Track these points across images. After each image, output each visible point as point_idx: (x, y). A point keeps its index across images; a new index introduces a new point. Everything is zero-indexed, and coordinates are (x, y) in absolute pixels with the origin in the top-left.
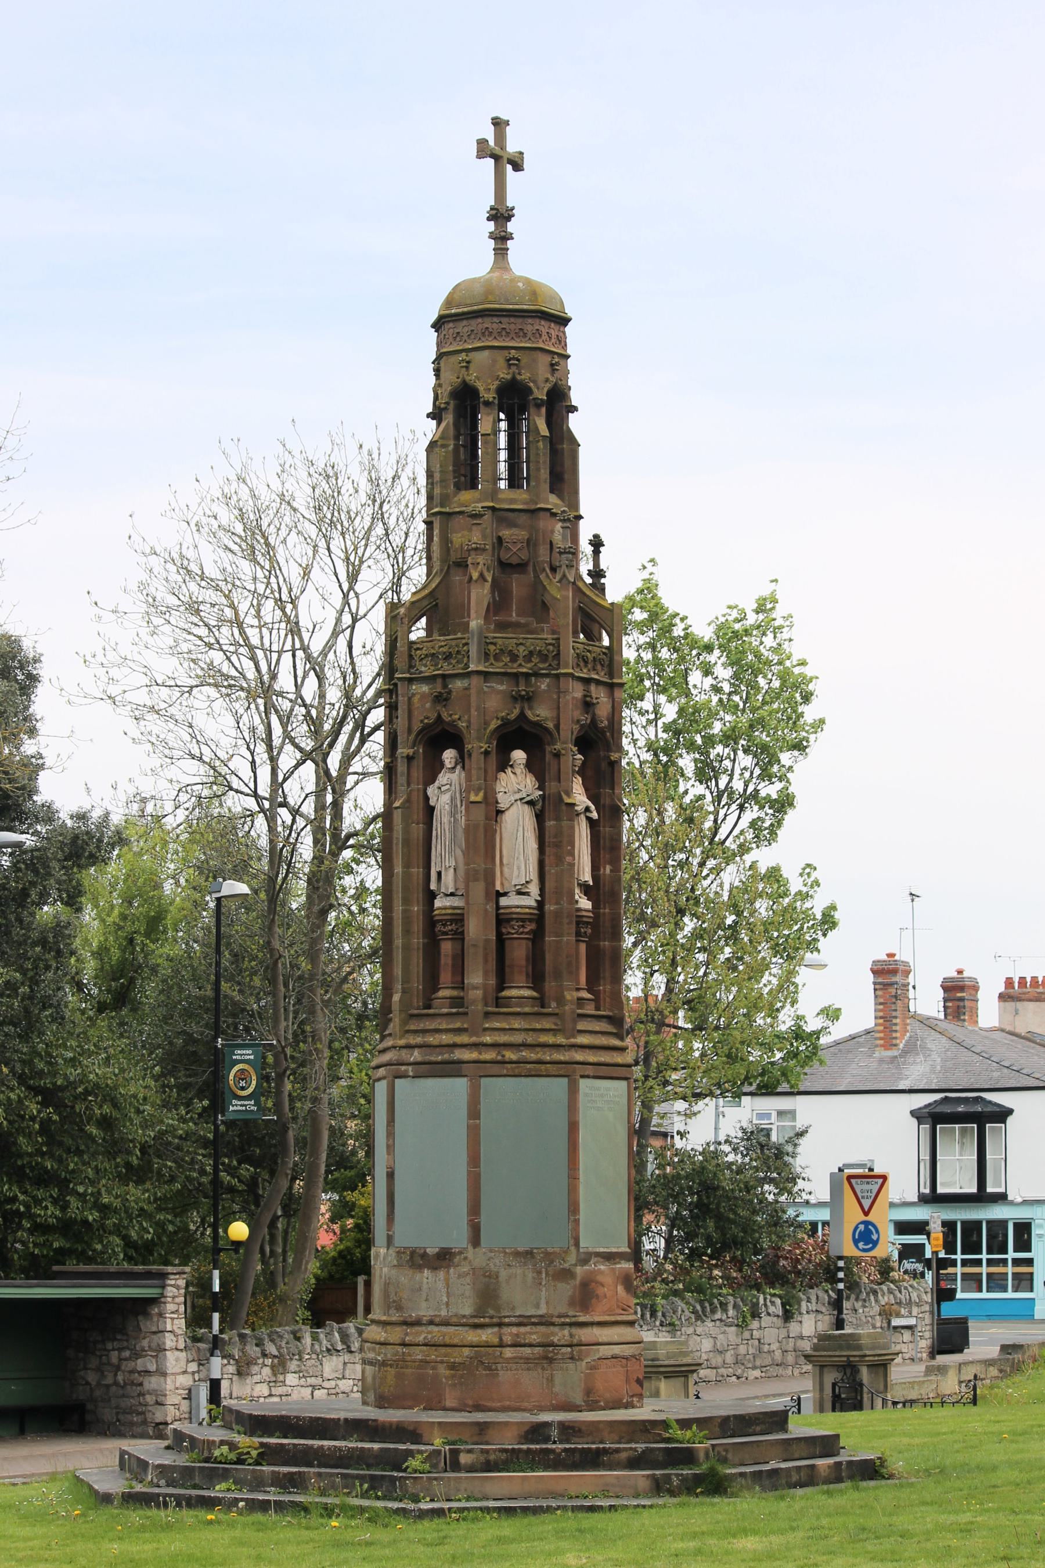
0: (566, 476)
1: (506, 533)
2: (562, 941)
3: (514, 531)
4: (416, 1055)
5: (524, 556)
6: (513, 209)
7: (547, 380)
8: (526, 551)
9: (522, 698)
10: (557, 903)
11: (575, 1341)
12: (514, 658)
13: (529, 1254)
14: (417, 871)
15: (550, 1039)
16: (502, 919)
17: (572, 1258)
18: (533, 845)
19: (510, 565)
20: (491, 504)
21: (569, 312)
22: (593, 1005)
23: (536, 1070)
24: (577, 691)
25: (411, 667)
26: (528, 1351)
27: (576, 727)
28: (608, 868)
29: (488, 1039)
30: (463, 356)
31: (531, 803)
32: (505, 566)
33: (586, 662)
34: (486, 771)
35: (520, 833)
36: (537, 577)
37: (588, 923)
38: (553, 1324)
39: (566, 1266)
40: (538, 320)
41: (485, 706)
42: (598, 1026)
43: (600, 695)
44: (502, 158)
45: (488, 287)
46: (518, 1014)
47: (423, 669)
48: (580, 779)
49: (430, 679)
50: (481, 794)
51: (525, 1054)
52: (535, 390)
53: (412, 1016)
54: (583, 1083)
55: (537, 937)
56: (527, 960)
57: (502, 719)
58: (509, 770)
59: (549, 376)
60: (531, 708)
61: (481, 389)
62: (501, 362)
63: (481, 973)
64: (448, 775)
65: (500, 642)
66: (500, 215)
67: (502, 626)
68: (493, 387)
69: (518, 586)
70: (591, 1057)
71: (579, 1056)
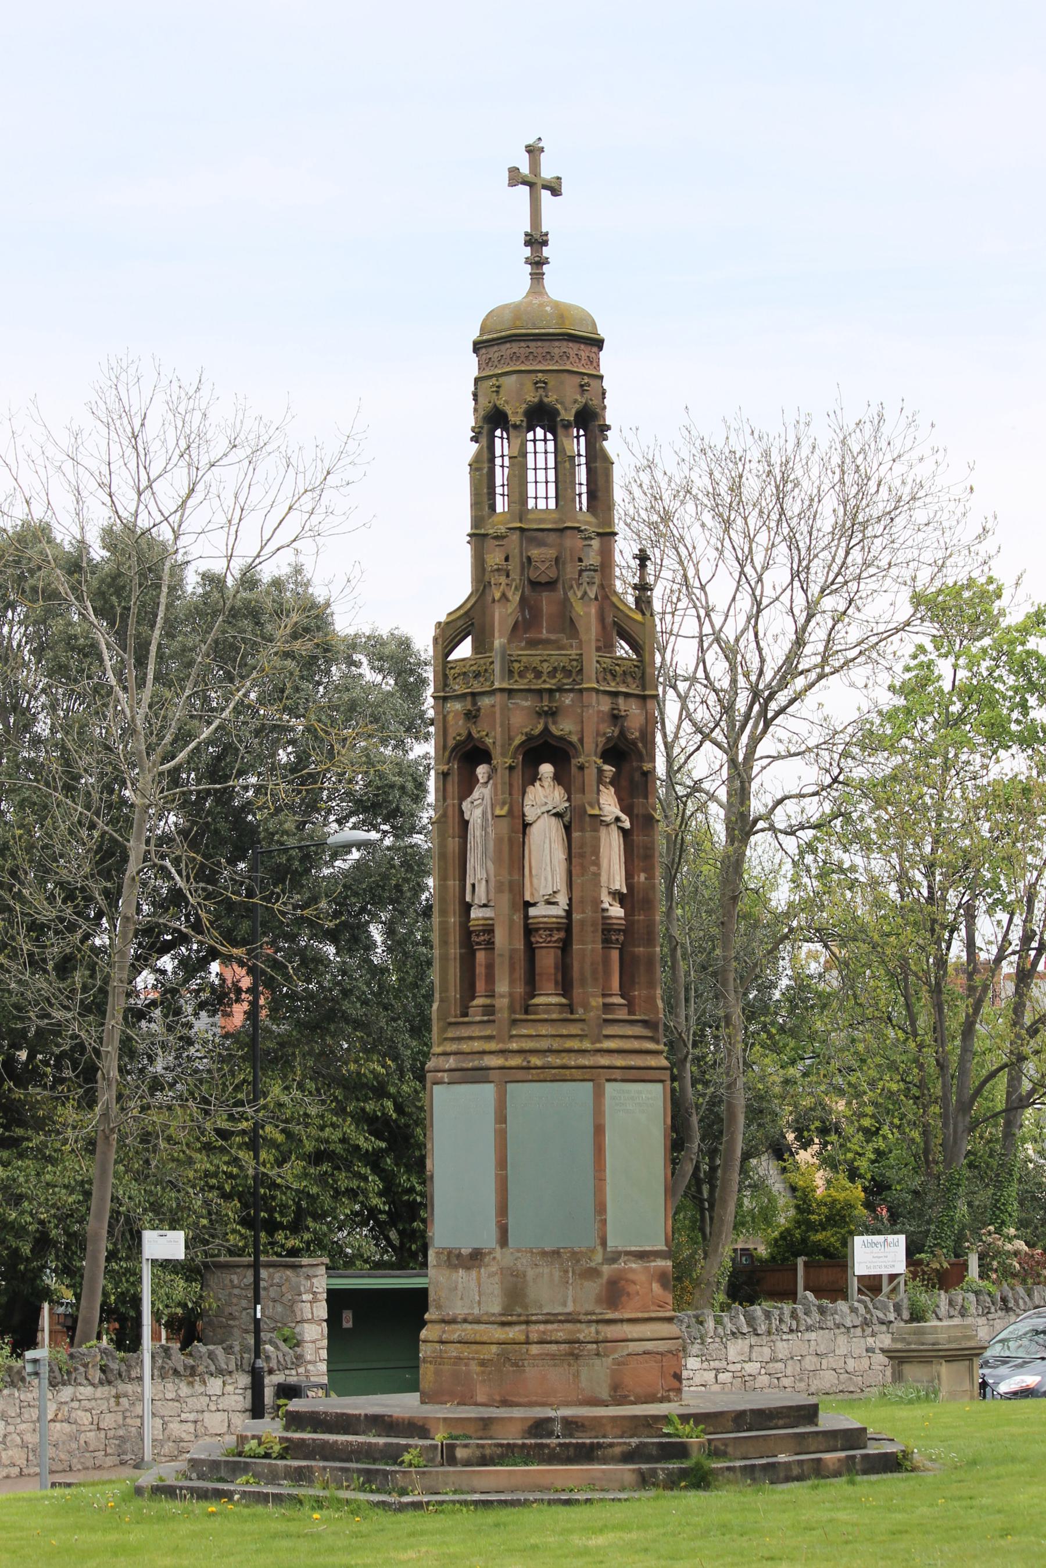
0: (600, 494)
1: (535, 552)
2: (587, 947)
3: (543, 550)
4: (451, 1062)
5: (553, 574)
6: (547, 234)
7: (575, 401)
8: (554, 568)
9: (546, 713)
10: (583, 912)
11: (601, 1338)
12: (538, 674)
13: (556, 1253)
14: (453, 884)
15: (575, 1044)
16: (529, 930)
17: (599, 1257)
18: (560, 855)
19: (539, 584)
20: (519, 525)
21: (602, 332)
22: (625, 1010)
23: (561, 1075)
24: (605, 705)
25: (446, 685)
26: (554, 1347)
27: (602, 740)
28: (642, 877)
29: (514, 1046)
30: (494, 381)
31: (557, 815)
32: (535, 585)
33: (614, 676)
34: (511, 785)
35: (547, 845)
36: (565, 594)
37: (620, 930)
38: (580, 1322)
39: (593, 1264)
40: (565, 343)
41: (509, 722)
42: (629, 1030)
43: (632, 710)
44: (535, 182)
45: (517, 311)
46: (546, 1020)
47: (457, 687)
48: (612, 790)
49: (462, 697)
50: (506, 808)
51: (551, 1059)
52: (562, 412)
53: (450, 1024)
54: (609, 1087)
55: (566, 946)
56: (556, 968)
57: (526, 734)
58: (537, 784)
59: (578, 397)
60: (555, 723)
61: (509, 412)
62: (529, 386)
63: (507, 982)
64: (483, 790)
65: (524, 659)
66: (536, 241)
67: (532, 644)
68: (521, 411)
69: (547, 603)
70: (619, 1061)
71: (604, 1061)
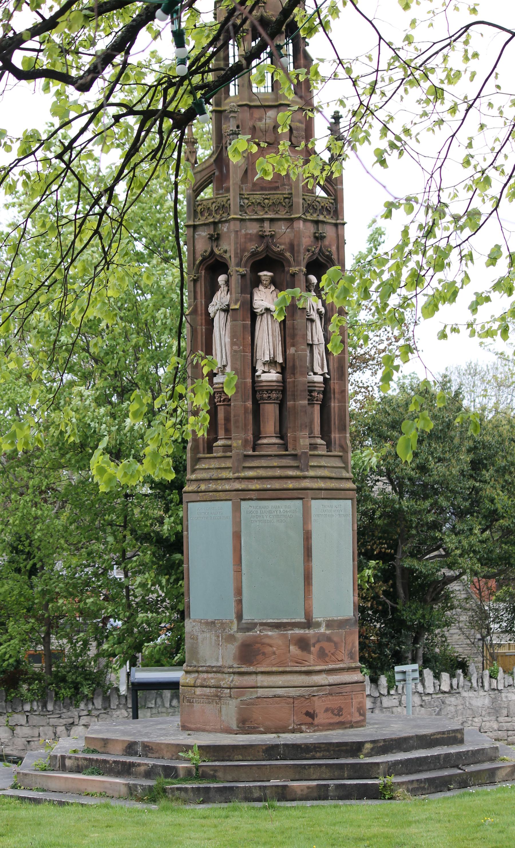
26: (208, 690)
38: (223, 673)
39: (232, 632)
